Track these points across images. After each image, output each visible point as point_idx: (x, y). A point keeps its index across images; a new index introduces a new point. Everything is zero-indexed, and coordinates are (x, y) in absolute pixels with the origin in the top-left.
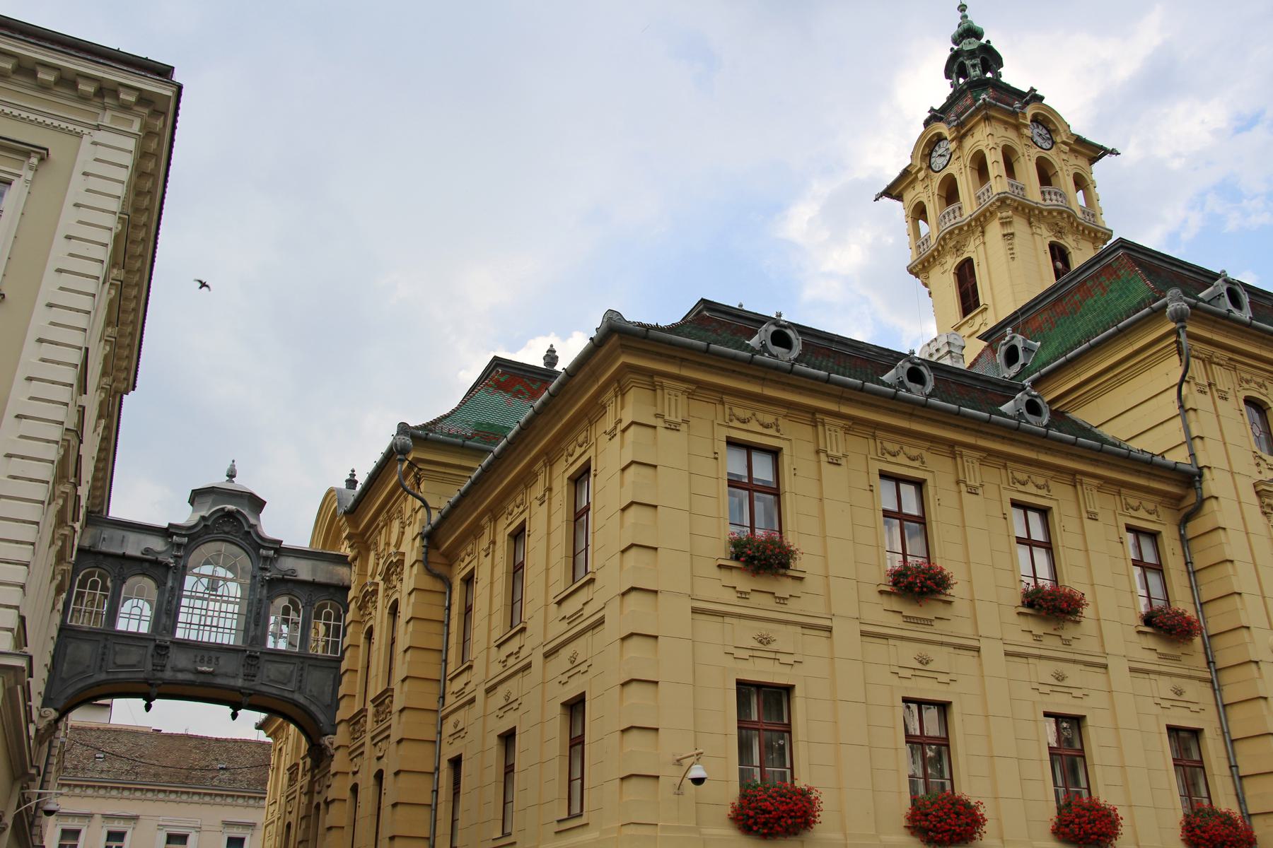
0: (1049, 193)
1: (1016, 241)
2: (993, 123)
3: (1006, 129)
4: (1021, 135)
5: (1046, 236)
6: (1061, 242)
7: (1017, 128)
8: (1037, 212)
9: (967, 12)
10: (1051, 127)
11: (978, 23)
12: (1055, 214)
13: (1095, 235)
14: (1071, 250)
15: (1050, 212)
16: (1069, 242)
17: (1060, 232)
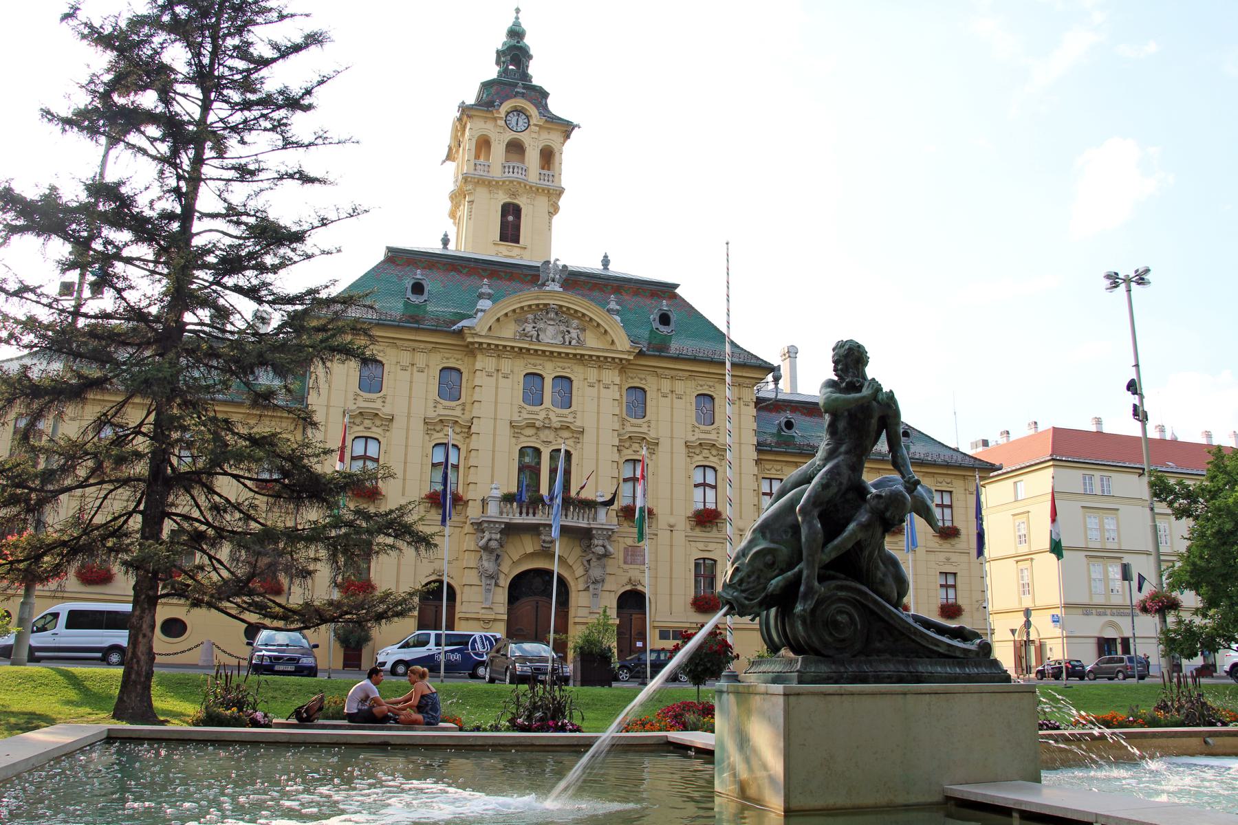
0: (509, 167)
1: (474, 206)
2: (475, 118)
3: (485, 122)
4: (496, 126)
5: (503, 198)
6: (515, 201)
7: (495, 119)
8: (494, 183)
9: (519, 15)
10: (529, 114)
11: (525, 25)
12: (515, 183)
13: (548, 191)
14: (522, 206)
15: (504, 182)
16: (522, 201)
17: (514, 195)
